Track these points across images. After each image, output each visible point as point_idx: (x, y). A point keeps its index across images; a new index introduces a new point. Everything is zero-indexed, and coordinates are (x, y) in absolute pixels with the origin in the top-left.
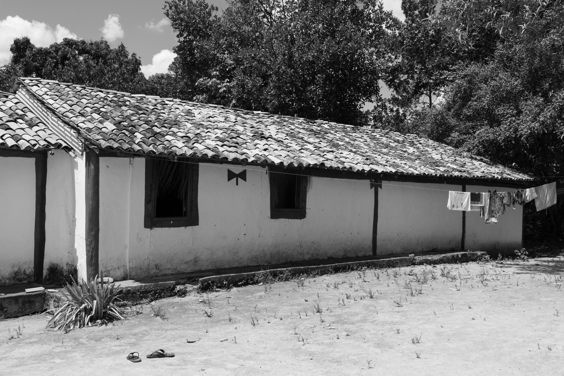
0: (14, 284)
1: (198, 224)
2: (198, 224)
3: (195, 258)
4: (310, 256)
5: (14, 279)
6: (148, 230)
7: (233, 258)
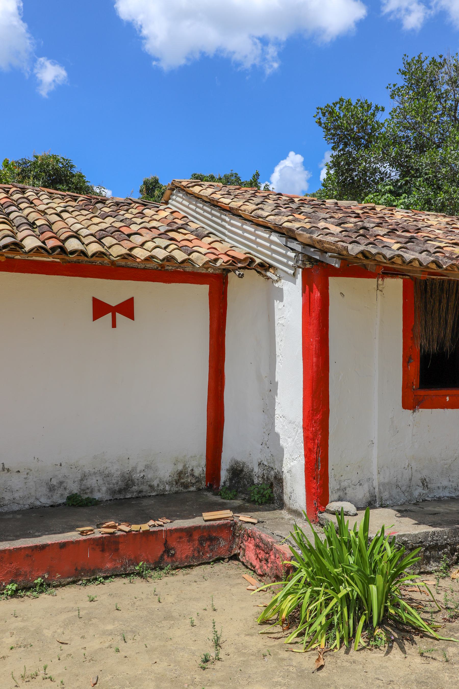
0: (177, 493)
5: (177, 483)
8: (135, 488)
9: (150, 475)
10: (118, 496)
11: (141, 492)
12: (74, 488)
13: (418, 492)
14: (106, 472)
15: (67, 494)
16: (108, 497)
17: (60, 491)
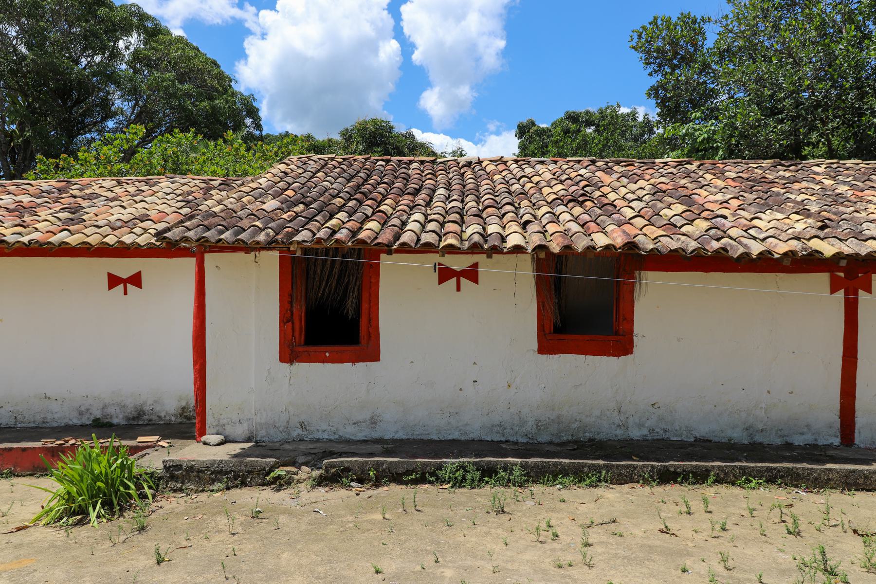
0: (181, 423)
1: (379, 360)
2: (379, 360)
3: (372, 417)
4: (645, 432)
6: (287, 365)
7: (449, 423)
8: (146, 417)
9: (158, 408)
10: (132, 422)
11: (151, 420)
12: (98, 414)
13: (296, 433)
14: (122, 404)
15: (92, 418)
16: (124, 423)
17: (87, 415)
